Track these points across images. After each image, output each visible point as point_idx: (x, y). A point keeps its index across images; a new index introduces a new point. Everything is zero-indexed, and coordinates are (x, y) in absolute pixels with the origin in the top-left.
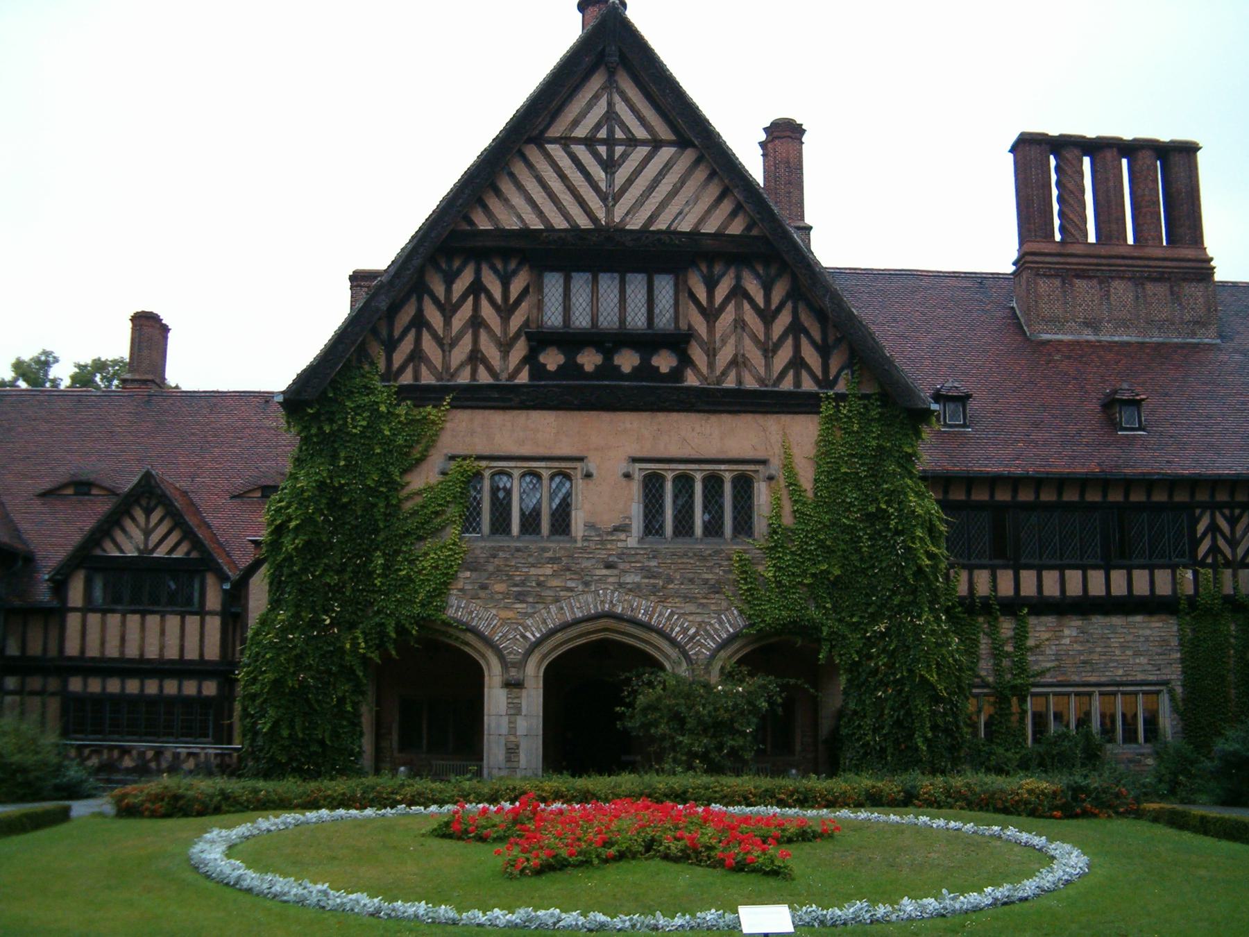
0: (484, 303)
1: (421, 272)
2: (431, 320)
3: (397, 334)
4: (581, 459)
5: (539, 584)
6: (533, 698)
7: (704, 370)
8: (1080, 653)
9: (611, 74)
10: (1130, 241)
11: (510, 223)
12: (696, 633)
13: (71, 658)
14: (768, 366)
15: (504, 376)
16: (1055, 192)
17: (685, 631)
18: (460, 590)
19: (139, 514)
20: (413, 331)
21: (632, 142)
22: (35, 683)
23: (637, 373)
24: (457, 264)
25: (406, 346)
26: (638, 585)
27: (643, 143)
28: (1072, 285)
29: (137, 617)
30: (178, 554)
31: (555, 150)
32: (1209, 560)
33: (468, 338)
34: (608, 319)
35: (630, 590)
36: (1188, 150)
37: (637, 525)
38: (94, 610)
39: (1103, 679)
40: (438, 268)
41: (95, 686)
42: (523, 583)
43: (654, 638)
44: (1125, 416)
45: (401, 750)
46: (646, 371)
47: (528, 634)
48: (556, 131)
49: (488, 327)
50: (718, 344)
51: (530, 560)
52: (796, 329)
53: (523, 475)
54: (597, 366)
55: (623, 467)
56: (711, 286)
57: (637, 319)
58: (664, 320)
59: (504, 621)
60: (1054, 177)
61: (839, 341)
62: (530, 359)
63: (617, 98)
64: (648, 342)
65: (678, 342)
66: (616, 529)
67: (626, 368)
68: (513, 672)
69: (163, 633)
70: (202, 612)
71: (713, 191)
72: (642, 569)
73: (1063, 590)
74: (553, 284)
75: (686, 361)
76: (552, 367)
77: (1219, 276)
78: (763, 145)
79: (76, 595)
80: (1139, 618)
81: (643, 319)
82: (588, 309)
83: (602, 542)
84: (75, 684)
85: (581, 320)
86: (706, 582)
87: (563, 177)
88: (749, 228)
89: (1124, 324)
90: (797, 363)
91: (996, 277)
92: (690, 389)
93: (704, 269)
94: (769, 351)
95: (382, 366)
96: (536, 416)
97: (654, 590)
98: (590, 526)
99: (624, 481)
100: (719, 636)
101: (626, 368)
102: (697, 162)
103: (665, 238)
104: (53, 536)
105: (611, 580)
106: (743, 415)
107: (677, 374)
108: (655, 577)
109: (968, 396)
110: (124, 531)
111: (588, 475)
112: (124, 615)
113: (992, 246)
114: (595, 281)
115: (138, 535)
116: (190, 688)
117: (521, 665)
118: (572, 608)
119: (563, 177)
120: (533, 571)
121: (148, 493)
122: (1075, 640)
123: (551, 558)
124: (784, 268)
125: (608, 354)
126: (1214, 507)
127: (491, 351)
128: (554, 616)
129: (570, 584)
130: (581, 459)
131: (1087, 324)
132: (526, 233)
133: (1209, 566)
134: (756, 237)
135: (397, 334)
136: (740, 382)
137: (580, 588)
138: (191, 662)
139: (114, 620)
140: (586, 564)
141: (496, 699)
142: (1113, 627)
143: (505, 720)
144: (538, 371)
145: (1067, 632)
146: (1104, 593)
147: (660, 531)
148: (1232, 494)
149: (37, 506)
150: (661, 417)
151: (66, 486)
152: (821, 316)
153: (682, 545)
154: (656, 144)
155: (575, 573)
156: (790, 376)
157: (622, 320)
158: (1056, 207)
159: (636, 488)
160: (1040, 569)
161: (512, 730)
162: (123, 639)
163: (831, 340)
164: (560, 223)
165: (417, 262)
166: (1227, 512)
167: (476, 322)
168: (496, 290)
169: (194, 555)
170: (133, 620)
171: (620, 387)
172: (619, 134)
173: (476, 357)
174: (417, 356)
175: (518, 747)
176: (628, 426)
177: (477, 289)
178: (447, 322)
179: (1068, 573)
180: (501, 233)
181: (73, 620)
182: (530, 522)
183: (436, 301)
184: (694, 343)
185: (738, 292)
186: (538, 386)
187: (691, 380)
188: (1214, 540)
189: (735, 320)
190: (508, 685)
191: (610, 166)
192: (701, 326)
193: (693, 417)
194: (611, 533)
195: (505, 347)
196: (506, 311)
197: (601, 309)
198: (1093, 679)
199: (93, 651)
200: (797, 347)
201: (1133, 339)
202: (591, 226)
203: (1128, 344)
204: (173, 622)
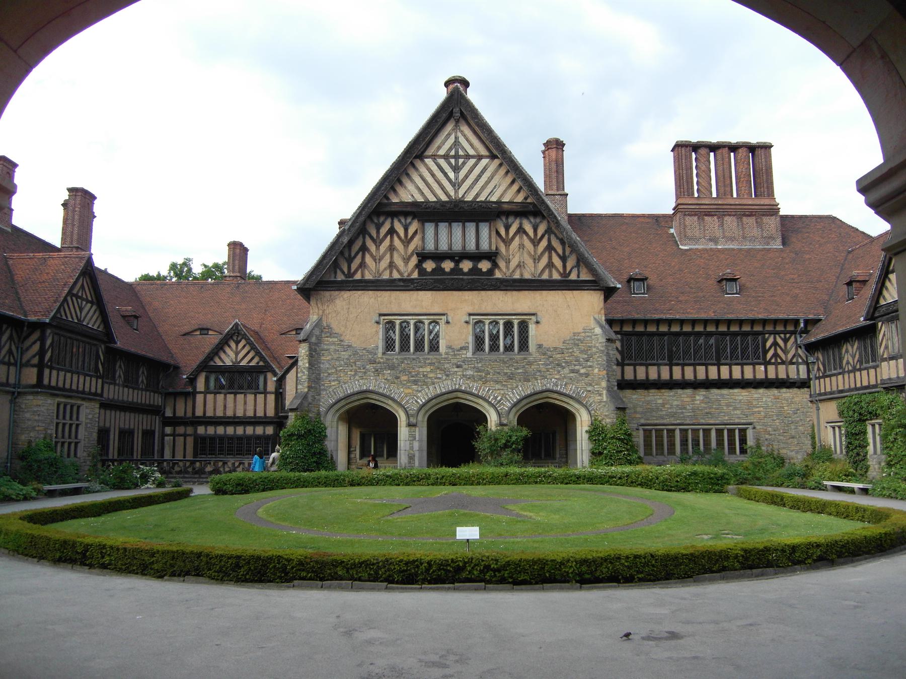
0: (396, 238)
1: (364, 223)
3: (353, 254)
6: (422, 432)
7: (504, 269)
8: (705, 408)
9: (457, 122)
10: (735, 195)
11: (409, 199)
12: (501, 399)
15: (406, 274)
16: (695, 172)
19: (233, 345)
20: (361, 253)
21: (468, 157)
22: (181, 430)
24: (382, 219)
27: (473, 157)
28: (703, 219)
29: (232, 396)
30: (253, 364)
31: (429, 161)
32: (773, 361)
33: (388, 255)
34: (457, 247)
36: (767, 147)
38: (211, 393)
39: (717, 422)
40: (372, 221)
41: (211, 430)
42: (416, 375)
43: (481, 401)
44: (729, 286)
46: (475, 271)
48: (430, 152)
49: (397, 250)
52: (550, 248)
56: (507, 228)
57: (471, 246)
58: (485, 246)
60: (694, 164)
62: (419, 266)
63: (459, 134)
64: (476, 257)
65: (491, 256)
66: (462, 348)
67: (466, 270)
68: (413, 420)
69: (245, 403)
70: (265, 393)
71: (509, 179)
73: (695, 376)
74: (430, 228)
75: (495, 265)
76: (429, 270)
77: (782, 213)
78: (544, 152)
79: (200, 385)
80: (736, 391)
83: (455, 355)
84: (201, 430)
85: (444, 247)
87: (433, 175)
88: (526, 198)
89: (732, 239)
90: (550, 265)
91: (664, 216)
92: (497, 279)
93: (504, 219)
94: (536, 260)
96: (421, 293)
97: (481, 378)
98: (449, 347)
101: (466, 270)
102: (501, 165)
103: (484, 205)
104: (188, 357)
107: (491, 272)
108: (480, 371)
109: (646, 279)
110: (224, 352)
111: (448, 322)
112: (225, 395)
113: (662, 199)
114: (450, 225)
115: (232, 355)
116: (259, 430)
119: (433, 175)
120: (421, 370)
121: (235, 334)
122: (702, 402)
124: (544, 217)
125: (457, 262)
126: (776, 333)
128: (431, 392)
131: (711, 240)
132: (415, 204)
133: (773, 364)
134: (530, 203)
135: (353, 254)
138: (260, 417)
139: (220, 397)
141: (403, 432)
142: (722, 395)
144: (422, 272)
145: (698, 398)
146: (717, 378)
147: (483, 350)
148: (785, 326)
150: (483, 293)
151: (196, 330)
152: (562, 242)
153: (494, 356)
154: (480, 158)
155: (441, 370)
156: (547, 271)
158: (695, 179)
160: (683, 365)
161: (412, 448)
162: (225, 406)
163: (567, 253)
164: (432, 198)
165: (362, 219)
166: (782, 336)
167: (392, 248)
168: (401, 232)
169: (261, 363)
170: (230, 397)
172: (461, 153)
173: (392, 265)
174: (363, 265)
177: (392, 232)
178: (378, 248)
179: (698, 368)
180: (402, 203)
181: (200, 398)
182: (419, 346)
185: (521, 230)
187: (498, 275)
188: (775, 350)
191: (456, 169)
192: (503, 248)
193: (499, 292)
194: (458, 351)
195: (406, 260)
196: (407, 242)
198: (712, 422)
199: (210, 413)
200: (550, 257)
201: (736, 247)
202: (447, 199)
203: (733, 250)
204: (250, 398)
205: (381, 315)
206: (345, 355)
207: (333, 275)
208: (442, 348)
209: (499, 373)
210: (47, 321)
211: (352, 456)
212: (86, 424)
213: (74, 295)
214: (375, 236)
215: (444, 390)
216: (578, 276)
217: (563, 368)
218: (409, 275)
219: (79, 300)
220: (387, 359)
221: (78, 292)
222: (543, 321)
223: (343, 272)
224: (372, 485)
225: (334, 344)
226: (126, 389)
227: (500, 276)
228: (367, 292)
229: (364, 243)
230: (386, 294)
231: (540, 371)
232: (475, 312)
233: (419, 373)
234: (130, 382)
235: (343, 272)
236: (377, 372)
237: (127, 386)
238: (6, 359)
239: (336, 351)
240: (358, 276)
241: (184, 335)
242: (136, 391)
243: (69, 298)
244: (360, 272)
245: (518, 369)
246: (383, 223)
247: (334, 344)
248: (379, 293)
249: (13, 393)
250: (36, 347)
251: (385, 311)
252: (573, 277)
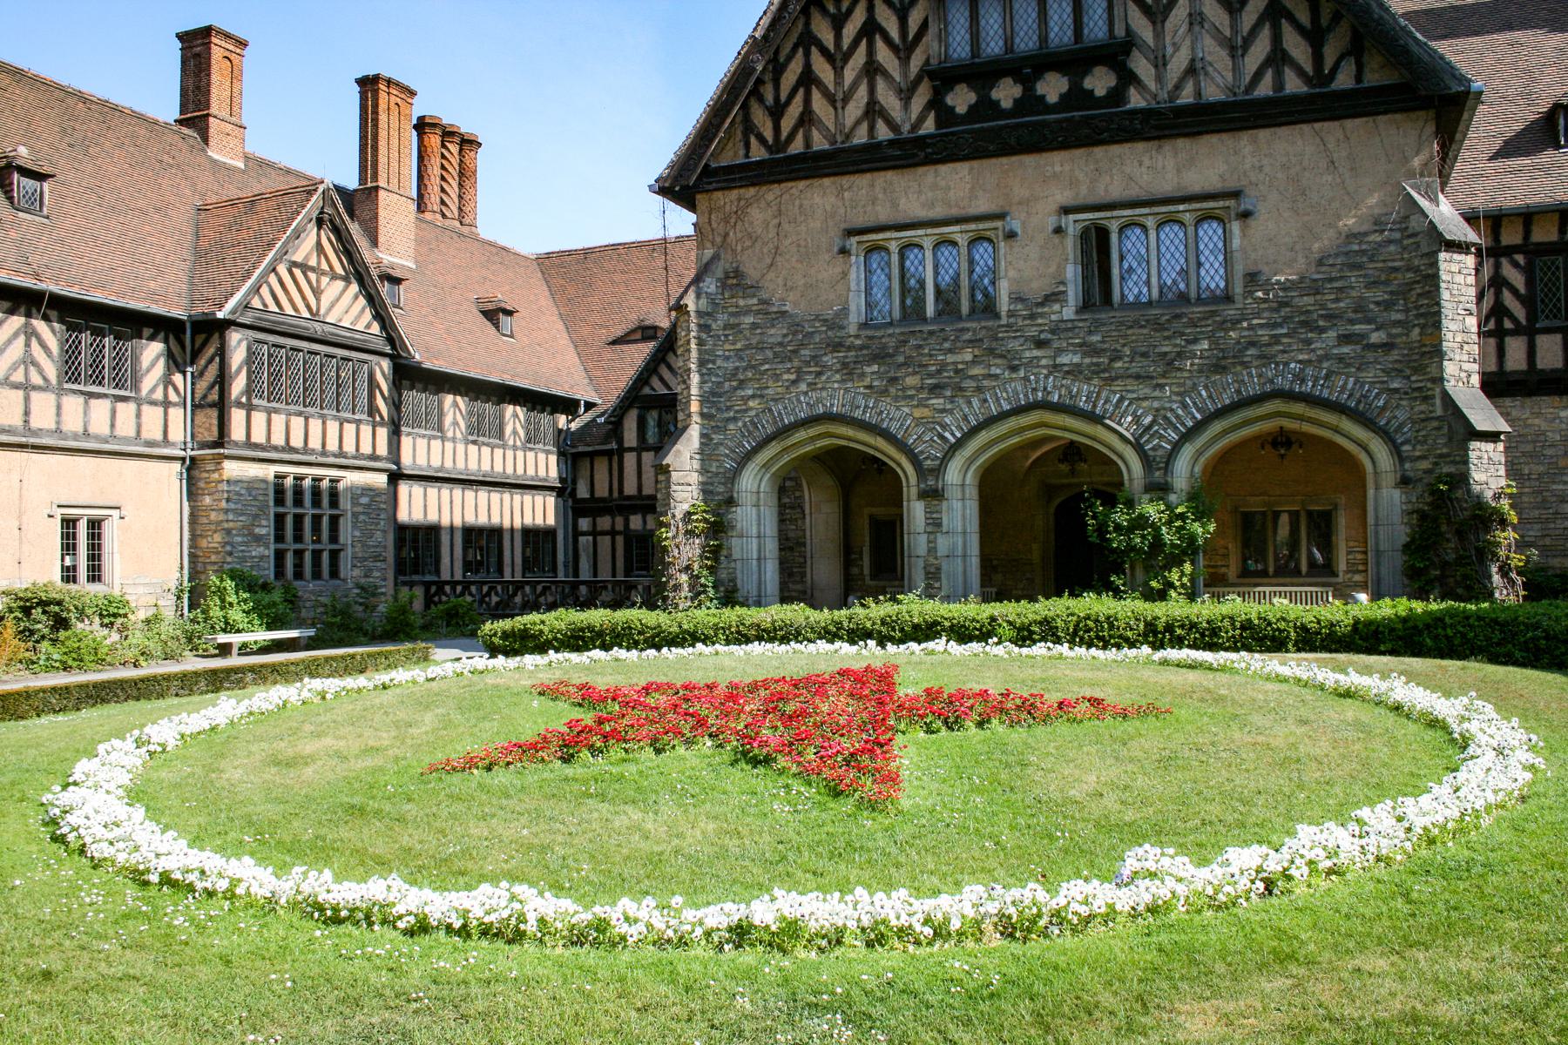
2: (821, 75)
3: (783, 97)
4: (1001, 216)
7: (1152, 85)
12: (1154, 422)
13: (629, 498)
14: (1236, 70)
15: (906, 128)
17: (1137, 419)
18: (866, 387)
20: (801, 92)
22: (604, 522)
23: (1067, 101)
25: (795, 110)
26: (1078, 365)
33: (863, 90)
34: (1027, 41)
35: (1068, 372)
37: (1073, 294)
38: (648, 450)
40: (824, 11)
42: (939, 372)
45: (873, 577)
46: (1077, 97)
47: (947, 435)
49: (886, 74)
50: (1169, 50)
51: (947, 345)
53: (937, 246)
54: (1016, 101)
55: (1052, 222)
58: (1096, 29)
59: (918, 422)
61: (1337, 18)
62: (936, 103)
64: (1076, 61)
65: (1116, 54)
67: (1052, 98)
72: (1081, 345)
75: (1128, 78)
76: (961, 109)
79: (630, 437)
81: (1070, 33)
82: (1000, 31)
83: (1032, 317)
85: (993, 46)
90: (1278, 58)
92: (1134, 112)
95: (768, 135)
96: (944, 169)
97: (1097, 370)
98: (1017, 298)
99: (1056, 239)
100: (1183, 424)
101: (1052, 98)
105: (1044, 362)
106: (1207, 137)
107: (1117, 95)
110: (670, 367)
111: (1011, 235)
117: (939, 471)
118: (998, 399)
120: (950, 358)
123: (970, 341)
125: (1028, 83)
127: (888, 99)
128: (975, 410)
129: (994, 370)
130: (1001, 216)
135: (783, 97)
136: (1198, 94)
140: (1014, 345)
143: (923, 539)
144: (945, 116)
149: (609, 353)
150: (1099, 151)
151: (633, 331)
156: (1268, 77)
157: (1043, 38)
159: (1070, 244)
161: (932, 550)
163: (1324, 22)
167: (872, 70)
171: (1044, 124)
173: (873, 110)
175: (939, 569)
176: (1058, 168)
177: (871, 29)
181: (630, 460)
183: (824, 51)
184: (1135, 53)
186: (946, 135)
187: (1136, 100)
189: (1190, 15)
190: (924, 495)
192: (1143, 29)
193: (1140, 146)
194: (1042, 304)
195: (906, 95)
196: (903, 51)
197: (1017, 29)
200: (1277, 39)
205: (851, 232)
206: (776, 333)
207: (742, 152)
208: (1004, 305)
209: (1144, 355)
210: (220, 315)
211: (855, 571)
212: (354, 514)
213: (295, 264)
214: (831, 47)
215: (1006, 407)
216: (1359, 79)
217: (1322, 330)
218: (915, 127)
219: (313, 276)
220: (871, 338)
221: (307, 257)
222: (1262, 210)
223: (762, 140)
224: (771, 640)
225: (747, 311)
226: (473, 449)
227: (1143, 104)
228: (816, 182)
229: (808, 66)
230: (863, 180)
231: (1252, 344)
232: (1080, 201)
233: (943, 367)
234: (484, 431)
235: (762, 140)
236: (849, 371)
237: (474, 442)
238: (159, 395)
239: (754, 326)
240: (797, 147)
241: (614, 343)
242: (499, 452)
243: (282, 269)
244: (800, 136)
245: (1195, 341)
246: (850, 11)
247: (747, 311)
248: (845, 181)
249: (183, 459)
250: (213, 370)
251: (860, 221)
252: (1344, 80)
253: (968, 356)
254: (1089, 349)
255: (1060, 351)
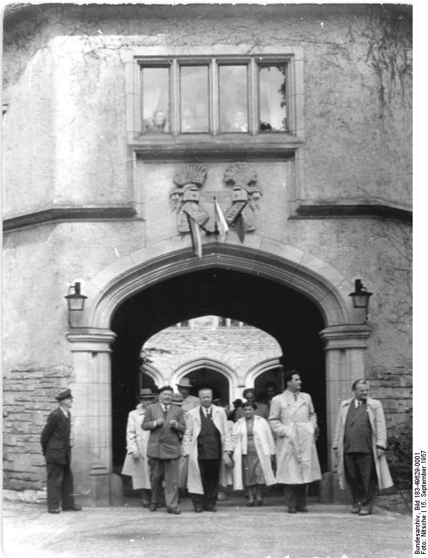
5: (177, 346)
51: (173, 337)
86: (243, 345)
120: (174, 341)
128: (183, 359)
129: (189, 346)
137: (193, 348)
140: (194, 338)
194: (204, 325)
209: (238, 344)
233: (172, 343)
245: (254, 340)
253: (180, 341)
254: (220, 341)
255: (211, 341)
